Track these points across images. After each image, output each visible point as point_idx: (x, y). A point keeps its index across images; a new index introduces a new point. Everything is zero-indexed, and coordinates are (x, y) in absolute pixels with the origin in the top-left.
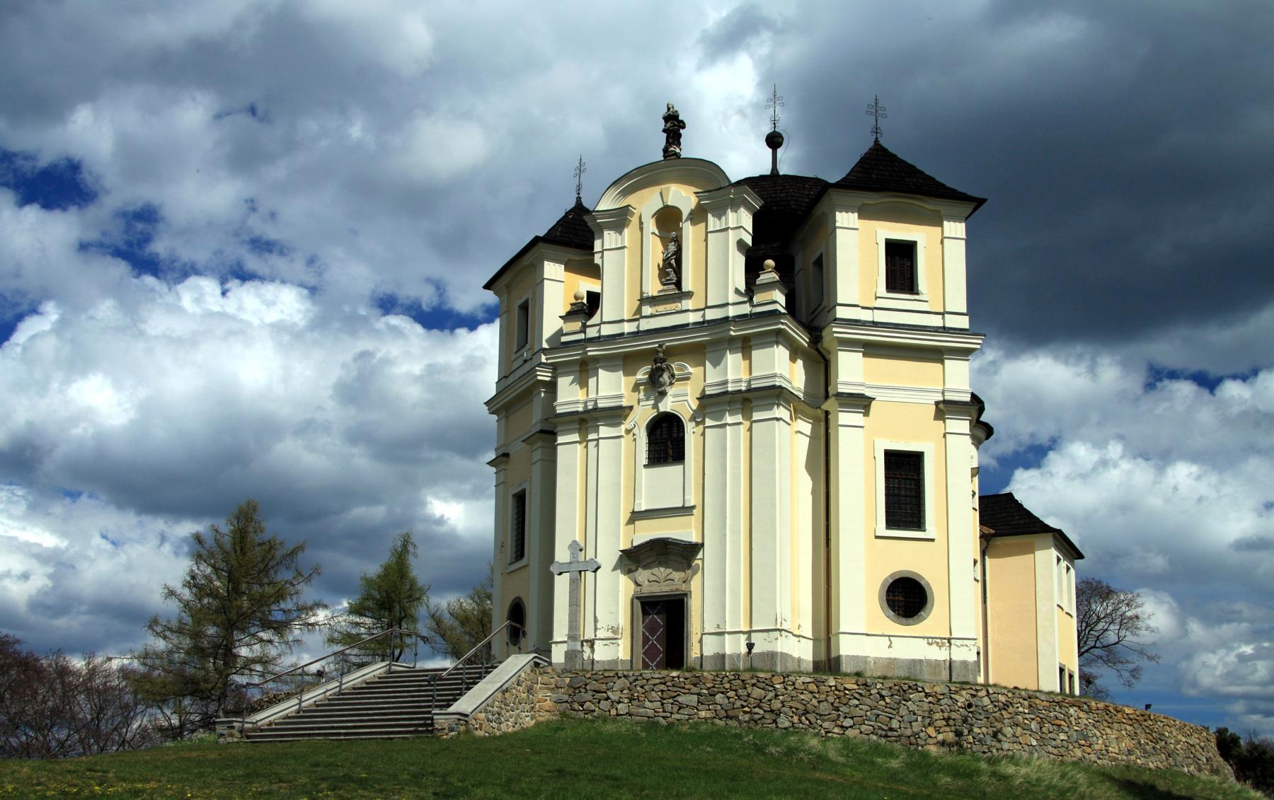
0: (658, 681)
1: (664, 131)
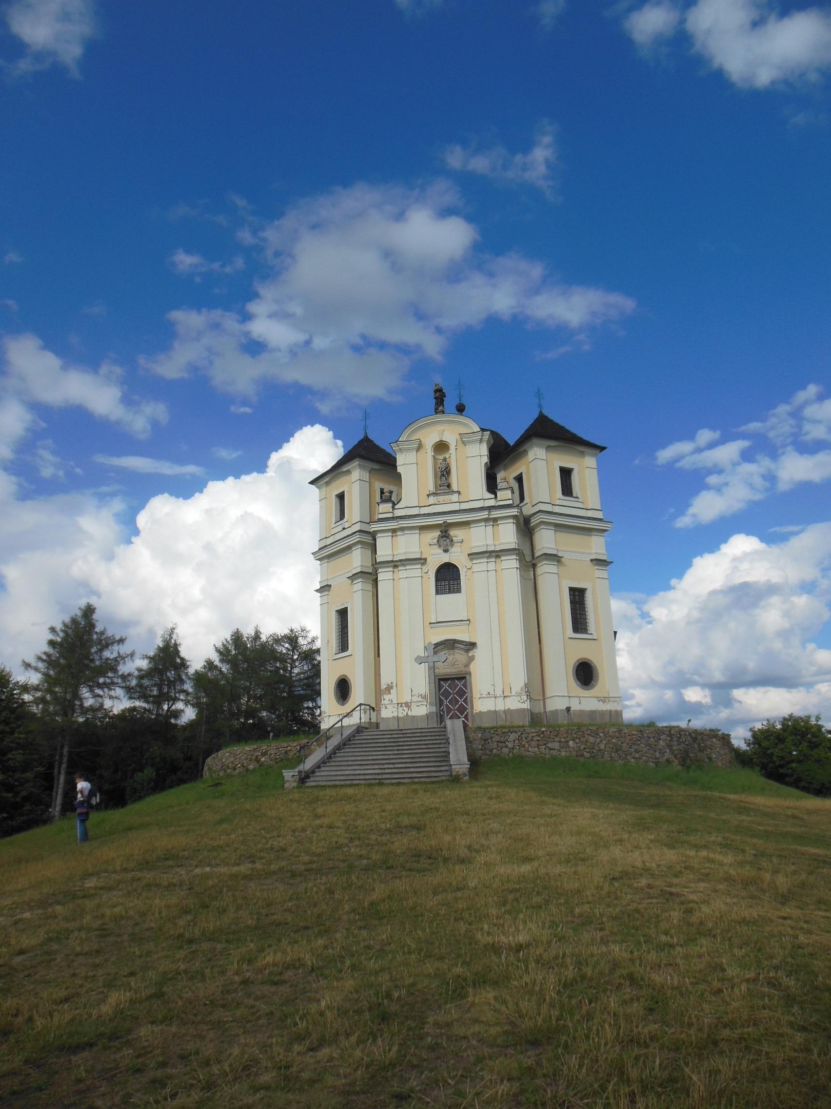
0: (535, 734)
1: (435, 398)
